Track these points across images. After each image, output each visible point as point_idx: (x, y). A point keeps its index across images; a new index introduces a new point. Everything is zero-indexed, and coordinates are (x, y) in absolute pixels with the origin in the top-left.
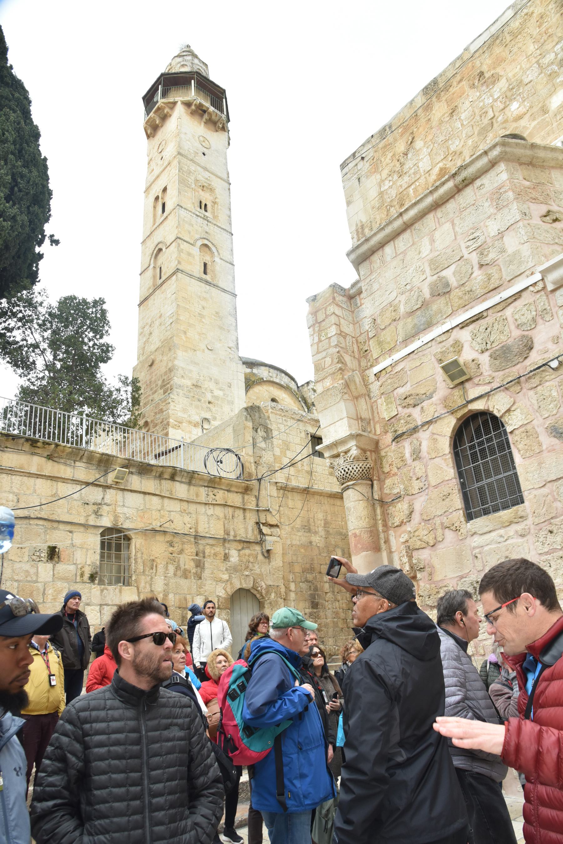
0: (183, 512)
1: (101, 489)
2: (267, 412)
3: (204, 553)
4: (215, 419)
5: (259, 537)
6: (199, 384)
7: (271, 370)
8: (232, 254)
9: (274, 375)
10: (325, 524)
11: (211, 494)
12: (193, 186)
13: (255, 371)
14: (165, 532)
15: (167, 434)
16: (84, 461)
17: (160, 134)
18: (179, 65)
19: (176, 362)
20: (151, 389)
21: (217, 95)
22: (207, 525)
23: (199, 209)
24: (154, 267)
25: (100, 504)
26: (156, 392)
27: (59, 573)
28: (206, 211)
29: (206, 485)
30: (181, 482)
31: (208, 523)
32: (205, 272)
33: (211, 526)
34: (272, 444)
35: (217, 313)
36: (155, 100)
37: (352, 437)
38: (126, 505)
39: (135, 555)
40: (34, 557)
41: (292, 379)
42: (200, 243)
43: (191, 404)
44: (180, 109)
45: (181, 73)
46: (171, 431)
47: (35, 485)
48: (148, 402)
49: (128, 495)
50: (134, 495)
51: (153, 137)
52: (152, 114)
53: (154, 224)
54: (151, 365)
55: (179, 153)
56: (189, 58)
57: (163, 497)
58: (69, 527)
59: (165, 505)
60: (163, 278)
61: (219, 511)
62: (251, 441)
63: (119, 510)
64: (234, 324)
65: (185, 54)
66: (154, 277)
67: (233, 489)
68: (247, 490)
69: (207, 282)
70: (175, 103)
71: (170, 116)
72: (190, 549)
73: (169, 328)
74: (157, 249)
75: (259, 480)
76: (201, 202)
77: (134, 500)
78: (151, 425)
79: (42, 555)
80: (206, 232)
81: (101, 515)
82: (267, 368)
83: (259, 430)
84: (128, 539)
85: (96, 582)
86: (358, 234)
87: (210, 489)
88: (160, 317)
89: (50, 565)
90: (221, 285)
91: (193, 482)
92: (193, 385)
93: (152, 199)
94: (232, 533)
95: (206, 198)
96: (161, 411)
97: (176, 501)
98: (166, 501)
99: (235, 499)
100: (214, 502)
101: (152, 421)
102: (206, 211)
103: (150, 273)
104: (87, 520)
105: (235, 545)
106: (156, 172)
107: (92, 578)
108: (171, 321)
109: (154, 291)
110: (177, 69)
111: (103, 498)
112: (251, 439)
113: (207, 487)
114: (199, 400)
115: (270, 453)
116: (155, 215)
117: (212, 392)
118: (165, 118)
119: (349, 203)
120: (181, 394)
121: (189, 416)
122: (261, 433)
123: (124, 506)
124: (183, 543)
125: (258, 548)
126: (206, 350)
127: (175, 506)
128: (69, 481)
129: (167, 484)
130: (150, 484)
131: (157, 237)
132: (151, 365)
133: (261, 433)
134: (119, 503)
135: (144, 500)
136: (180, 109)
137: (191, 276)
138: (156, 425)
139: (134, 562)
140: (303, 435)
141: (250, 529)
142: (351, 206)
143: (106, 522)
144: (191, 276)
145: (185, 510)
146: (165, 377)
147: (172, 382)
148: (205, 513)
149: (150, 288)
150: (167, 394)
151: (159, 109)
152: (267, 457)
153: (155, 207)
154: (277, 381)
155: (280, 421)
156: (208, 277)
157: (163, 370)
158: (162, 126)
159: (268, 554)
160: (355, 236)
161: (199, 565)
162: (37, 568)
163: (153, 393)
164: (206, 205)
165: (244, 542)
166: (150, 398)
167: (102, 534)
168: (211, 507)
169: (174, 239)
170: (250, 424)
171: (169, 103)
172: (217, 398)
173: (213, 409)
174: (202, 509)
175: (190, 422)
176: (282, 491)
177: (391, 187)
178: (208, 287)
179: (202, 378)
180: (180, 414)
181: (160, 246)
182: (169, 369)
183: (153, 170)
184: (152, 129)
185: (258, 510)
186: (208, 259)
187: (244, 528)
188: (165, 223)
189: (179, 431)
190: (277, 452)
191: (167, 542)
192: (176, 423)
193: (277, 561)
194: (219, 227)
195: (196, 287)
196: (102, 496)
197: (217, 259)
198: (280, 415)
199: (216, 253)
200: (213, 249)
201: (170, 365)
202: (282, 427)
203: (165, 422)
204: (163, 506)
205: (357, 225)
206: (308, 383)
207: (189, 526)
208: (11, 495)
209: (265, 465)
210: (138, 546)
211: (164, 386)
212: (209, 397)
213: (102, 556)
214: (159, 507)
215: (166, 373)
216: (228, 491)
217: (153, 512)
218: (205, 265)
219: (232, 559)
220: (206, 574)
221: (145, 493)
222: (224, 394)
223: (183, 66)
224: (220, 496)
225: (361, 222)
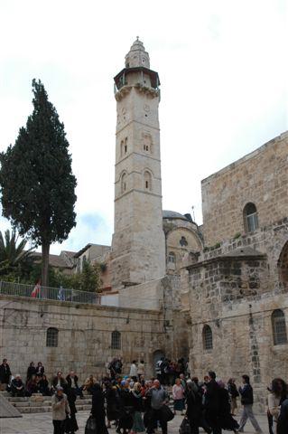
12: (141, 138)
13: (173, 222)
17: (123, 100)
21: (154, 77)
44: (133, 92)
68: (160, 313)
80: (148, 164)
84: (120, 334)
95: (147, 142)
99: (156, 317)
103: (119, 185)
119: (203, 201)
122: (167, 289)
125: (164, 335)
131: (124, 165)
136: (133, 92)
137: (140, 192)
143: (113, 329)
144: (140, 192)
152: (169, 299)
156: (148, 190)
157: (127, 241)
159: (168, 337)
161: (143, 342)
180: (135, 264)
186: (147, 179)
193: (172, 339)
195: (143, 197)
220: (145, 345)
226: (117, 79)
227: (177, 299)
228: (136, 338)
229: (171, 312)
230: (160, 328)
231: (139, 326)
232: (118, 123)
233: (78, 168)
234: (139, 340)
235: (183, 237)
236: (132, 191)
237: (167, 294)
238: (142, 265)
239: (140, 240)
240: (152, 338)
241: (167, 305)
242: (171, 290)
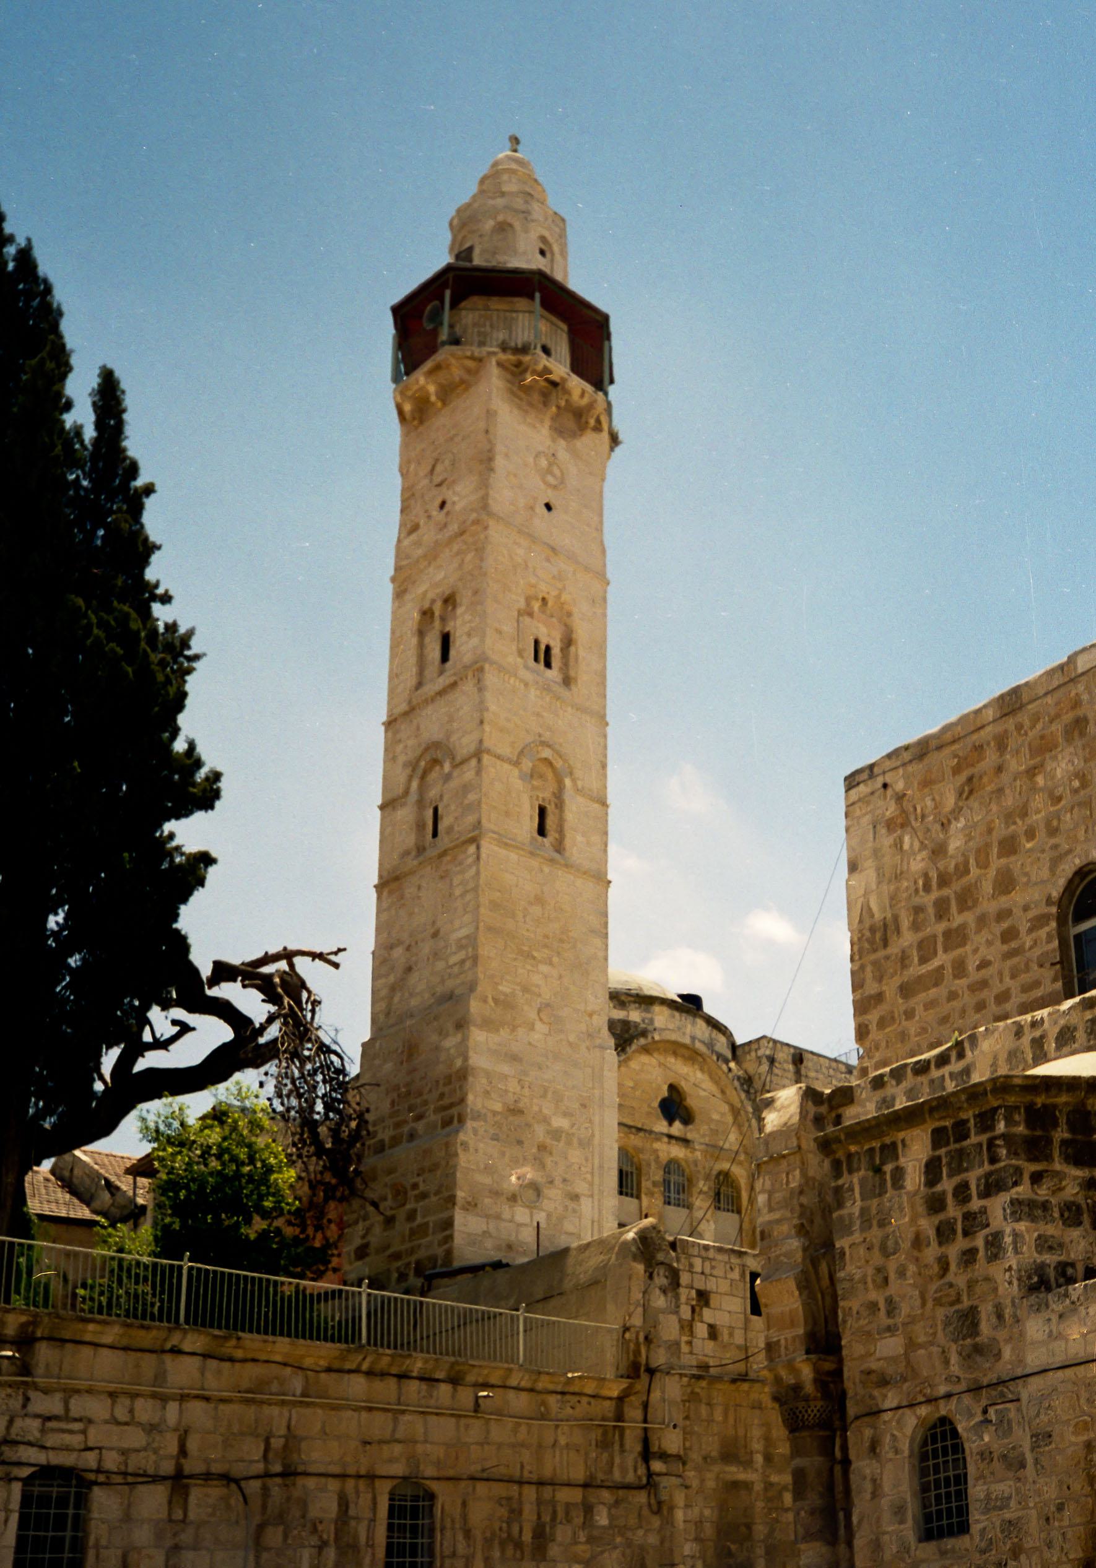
6: (521, 1105)
15: (449, 1224)
24: (420, 803)
26: (419, 1117)
43: (503, 1154)
66: (420, 826)
73: (456, 970)
78: (412, 1193)
106: (428, 535)
108: (462, 955)
114: (520, 1142)
117: (546, 1120)
119: (853, 867)
120: (481, 1132)
125: (641, 1498)
131: (431, 724)
138: (424, 1196)
142: (856, 875)
146: (446, 1090)
149: (407, 853)
152: (670, 1328)
153: (421, 634)
159: (660, 1508)
169: (472, 748)
170: (640, 1268)
173: (549, 1161)
179: (526, 1091)
188: (450, 697)
200: (559, 764)
201: (459, 1063)
222: (573, 1125)
230: (627, 1466)
235: (672, 1088)
236: (474, 840)
239: (505, 1069)
241: (660, 1358)
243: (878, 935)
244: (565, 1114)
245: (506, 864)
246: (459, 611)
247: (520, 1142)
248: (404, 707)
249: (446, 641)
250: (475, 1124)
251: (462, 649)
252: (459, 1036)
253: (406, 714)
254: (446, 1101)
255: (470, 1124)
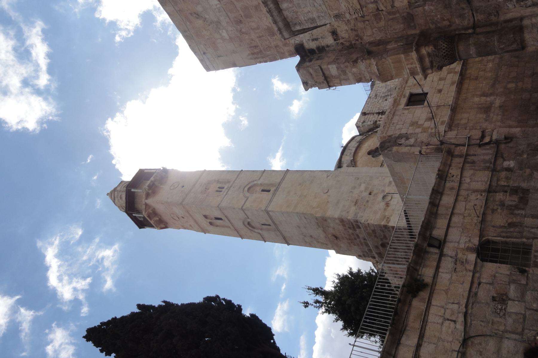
0: (466, 199)
1: (443, 258)
2: (385, 137)
3: (505, 186)
4: (383, 191)
5: (492, 145)
6: (355, 201)
7: (345, 153)
8: (257, 171)
9: (349, 151)
10: (484, 96)
11: (452, 179)
14: (484, 214)
16: (418, 268)
17: (165, 218)
18: (120, 201)
19: (336, 216)
20: (355, 239)
22: (479, 183)
23: (222, 193)
24: (261, 229)
25: (456, 260)
26: (358, 236)
27: (517, 297)
28: (223, 188)
29: (443, 182)
30: (440, 200)
31: (478, 182)
32: (269, 191)
33: (480, 180)
34: (412, 134)
35: (300, 184)
36: (142, 219)
37: (418, 51)
38: (457, 240)
39: (504, 237)
40: (502, 314)
41: (353, 138)
42: (247, 194)
44: (150, 201)
45: (126, 198)
46: (391, 224)
47: (437, 306)
48: (365, 243)
49: (449, 238)
50: (449, 234)
51: (167, 223)
52: (152, 222)
53: (229, 227)
54: (336, 238)
55: (181, 204)
56: (116, 193)
57: (452, 214)
58: (475, 285)
59: (459, 212)
60: (270, 222)
61: (468, 173)
62: (409, 148)
63: (462, 246)
64: (310, 172)
65: (113, 197)
66: (268, 230)
67: (449, 163)
68: (450, 153)
69: (276, 190)
70: (146, 205)
71: (154, 209)
72: (500, 196)
74: (248, 226)
75: (442, 143)
76: (217, 191)
77: (454, 234)
78: (385, 241)
79: (500, 307)
81: (466, 259)
82: (343, 156)
83: (400, 143)
84: (488, 242)
85: (527, 269)
86: (258, 58)
87: (448, 179)
88: (299, 227)
89: (510, 303)
90: (279, 180)
91: (441, 191)
92: (355, 205)
93: (211, 228)
94: (488, 165)
96: (374, 231)
97: (457, 204)
98: (456, 211)
99: (457, 162)
100: (459, 177)
101: (382, 240)
102: (223, 188)
104: (470, 271)
105: (500, 161)
107: (523, 272)
108: (303, 218)
109: (279, 231)
110: (123, 202)
111: (451, 257)
112: (407, 148)
113: (445, 181)
114: (368, 201)
115: (419, 136)
116: (223, 226)
118: (155, 213)
121: (380, 209)
122: (403, 141)
123: (458, 243)
124: (494, 201)
126: (328, 194)
127: (461, 207)
128: (435, 280)
129: (441, 210)
130: (441, 224)
131: (239, 225)
132: (336, 238)
133: (403, 141)
134: (456, 246)
135: (455, 227)
136: (150, 201)
137: (271, 201)
138: (385, 237)
139: (510, 239)
140: (406, 112)
141: (484, 151)
143: (472, 257)
145: (465, 198)
146: (347, 226)
147: (352, 221)
148: (469, 184)
150: (360, 225)
151: (149, 216)
152: (423, 137)
153: (217, 226)
154: (354, 149)
155: (393, 128)
156: (272, 189)
157: (341, 228)
158: (161, 216)
160: (259, 60)
162: (511, 313)
163: (358, 237)
164: (219, 188)
165: (496, 157)
166: (362, 241)
167: (483, 260)
168: (463, 179)
169: (242, 212)
170: (395, 149)
171: (145, 208)
172: (366, 189)
174: (465, 186)
175: (385, 209)
176: (452, 128)
177: (227, 31)
178: (279, 190)
180: (378, 216)
181: (246, 223)
182: (341, 222)
183: (191, 226)
184: (162, 224)
185: (468, 145)
186: (258, 189)
187: (485, 154)
189: (392, 218)
190: (419, 130)
191: (493, 212)
192: (385, 220)
193: (516, 131)
194: (236, 179)
196: (450, 259)
197: (259, 182)
198: (388, 128)
199: (255, 182)
201: (337, 221)
202: (398, 127)
203: (384, 229)
204: (460, 214)
205: (251, 59)
206: (358, 127)
207: (479, 196)
208: (444, 324)
209: (430, 139)
210: (495, 235)
211: (354, 227)
212: (366, 194)
213: (501, 263)
214: (461, 217)
215: (344, 225)
216: (450, 166)
217: (465, 221)
218: (263, 191)
219: (512, 166)
221: (449, 226)
222: (364, 183)
223: (121, 198)
224: (454, 171)
225: (249, 55)
226: (141, 224)
227: (427, 124)
228: (502, 204)
229: (452, 134)
231: (473, 197)
232: (190, 228)
233: (189, 292)
234: (511, 200)
235: (369, 153)
237: (412, 141)
238: (382, 205)
240: (508, 169)
242: (407, 137)
243: (256, 51)
244: (360, 185)
245: (279, 203)
246: (207, 214)
247: (368, 201)
248: (236, 232)
249: (217, 219)
250: (359, 216)
251: (218, 214)
252: (329, 221)
253: (238, 232)
254: (351, 226)
255: (359, 219)
